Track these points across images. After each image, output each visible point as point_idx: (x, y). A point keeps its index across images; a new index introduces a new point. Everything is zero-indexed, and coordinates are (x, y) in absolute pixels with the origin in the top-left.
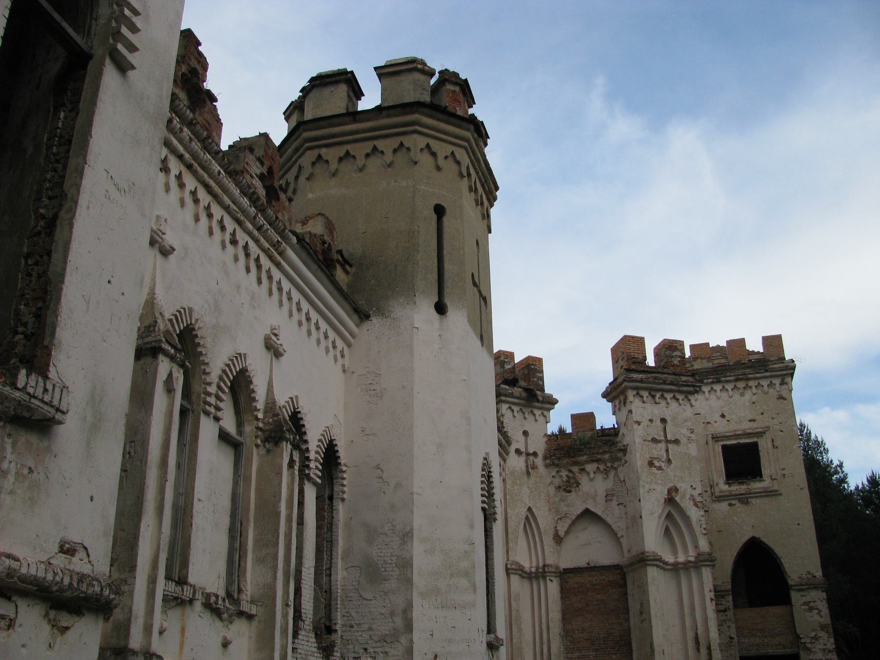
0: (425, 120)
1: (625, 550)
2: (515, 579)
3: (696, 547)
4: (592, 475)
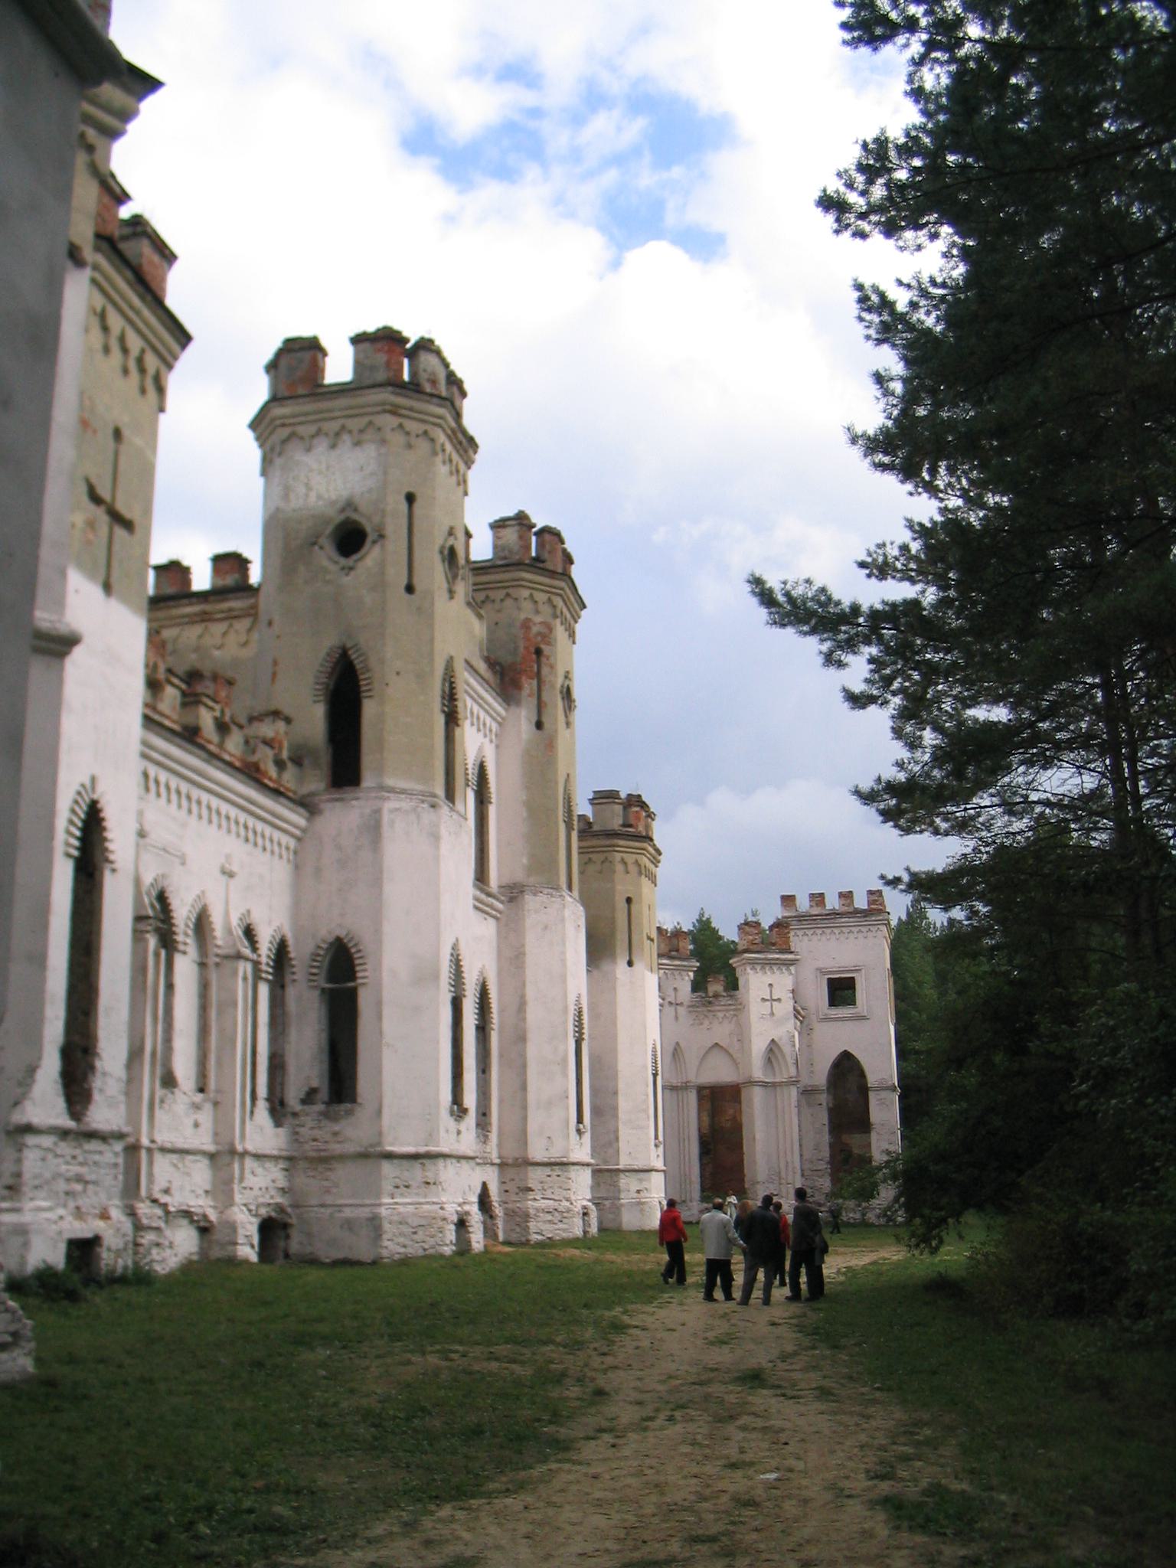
0: (621, 842)
2: (667, 1092)
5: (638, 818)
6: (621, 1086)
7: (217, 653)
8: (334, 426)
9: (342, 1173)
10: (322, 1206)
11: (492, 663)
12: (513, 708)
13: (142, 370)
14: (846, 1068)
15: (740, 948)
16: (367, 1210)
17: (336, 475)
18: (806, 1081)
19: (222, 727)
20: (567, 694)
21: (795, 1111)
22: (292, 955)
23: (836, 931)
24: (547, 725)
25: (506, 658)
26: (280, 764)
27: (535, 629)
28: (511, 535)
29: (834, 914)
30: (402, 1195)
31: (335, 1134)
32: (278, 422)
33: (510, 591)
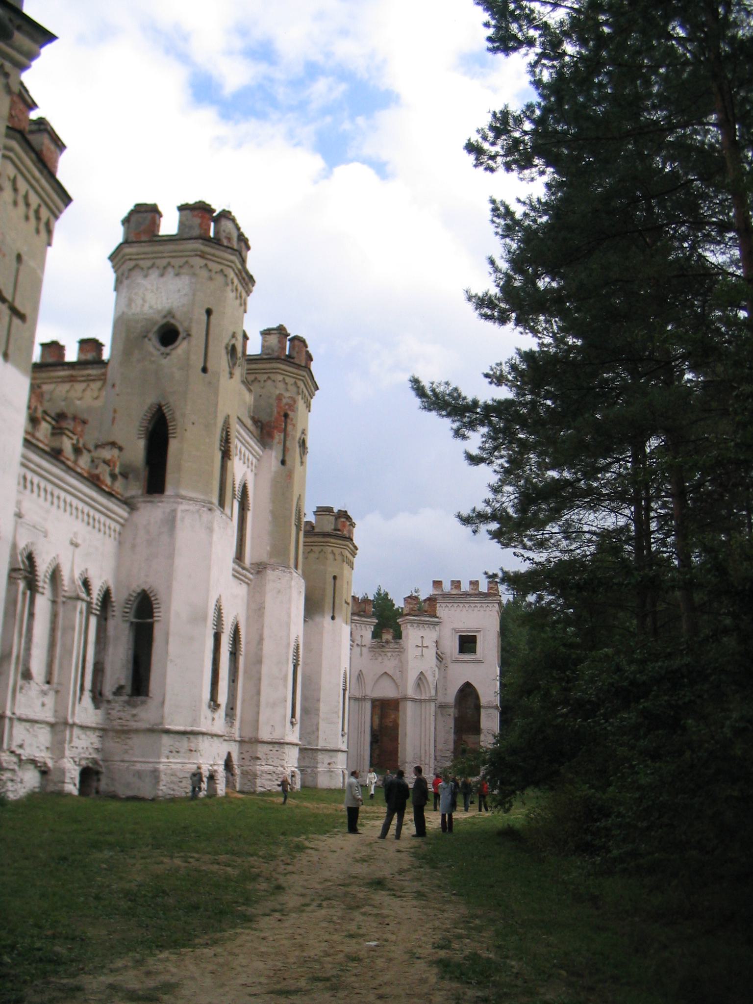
0: (332, 540)
2: (352, 701)
5: (344, 526)
6: (323, 696)
7: (78, 402)
8: (164, 262)
9: (137, 741)
10: (123, 761)
11: (255, 421)
12: (268, 451)
13: (38, 218)
14: (468, 693)
15: (405, 612)
16: (151, 765)
17: (163, 294)
18: (441, 699)
19: (77, 451)
20: (303, 444)
21: (433, 718)
22: (113, 599)
23: (467, 605)
24: (288, 462)
25: (264, 418)
26: (113, 476)
27: (284, 401)
28: (273, 340)
29: (466, 594)
30: (174, 757)
31: (134, 715)
32: (128, 257)
33: (271, 375)
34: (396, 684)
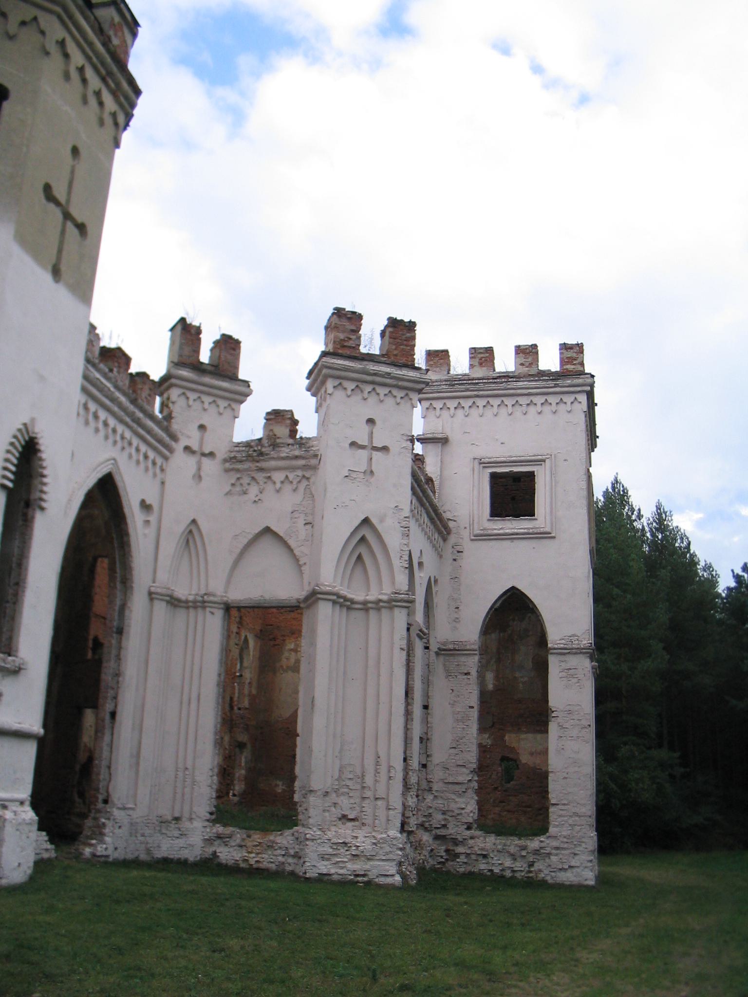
1: (306, 581)
2: (160, 607)
3: (393, 583)
4: (278, 485)
21: (400, 658)
23: (509, 401)
34: (296, 559)
